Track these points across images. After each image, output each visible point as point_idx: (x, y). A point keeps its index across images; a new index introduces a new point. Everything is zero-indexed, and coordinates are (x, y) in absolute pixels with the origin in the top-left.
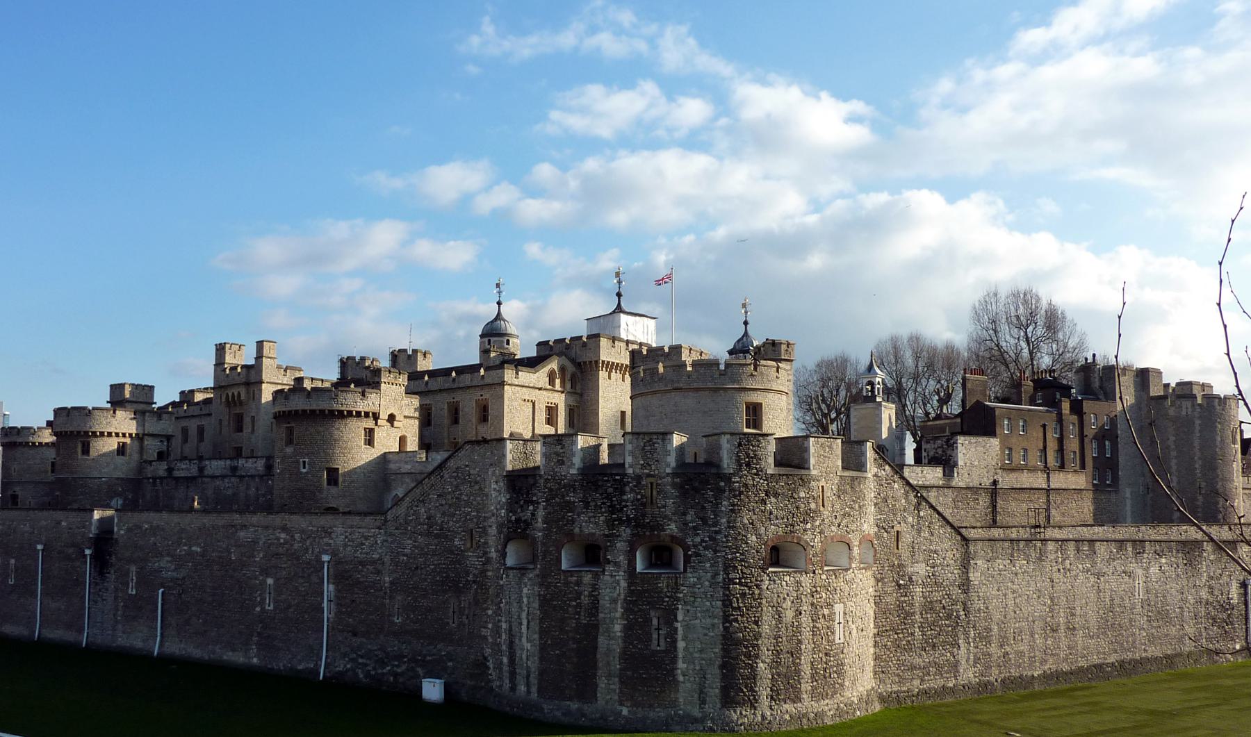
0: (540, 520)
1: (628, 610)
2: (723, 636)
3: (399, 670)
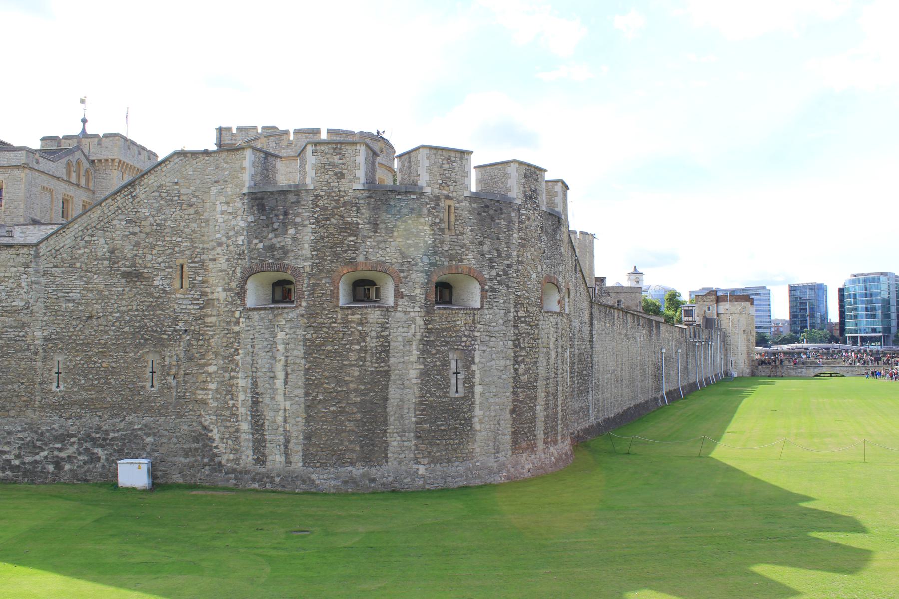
0: (307, 246)
1: (424, 353)
2: (514, 378)
3: (63, 455)
